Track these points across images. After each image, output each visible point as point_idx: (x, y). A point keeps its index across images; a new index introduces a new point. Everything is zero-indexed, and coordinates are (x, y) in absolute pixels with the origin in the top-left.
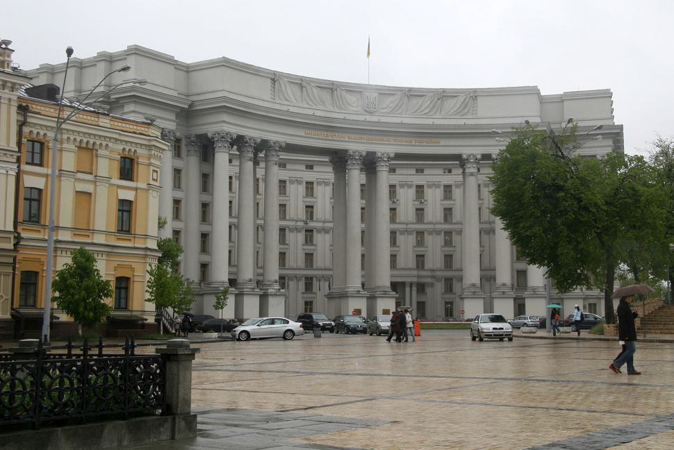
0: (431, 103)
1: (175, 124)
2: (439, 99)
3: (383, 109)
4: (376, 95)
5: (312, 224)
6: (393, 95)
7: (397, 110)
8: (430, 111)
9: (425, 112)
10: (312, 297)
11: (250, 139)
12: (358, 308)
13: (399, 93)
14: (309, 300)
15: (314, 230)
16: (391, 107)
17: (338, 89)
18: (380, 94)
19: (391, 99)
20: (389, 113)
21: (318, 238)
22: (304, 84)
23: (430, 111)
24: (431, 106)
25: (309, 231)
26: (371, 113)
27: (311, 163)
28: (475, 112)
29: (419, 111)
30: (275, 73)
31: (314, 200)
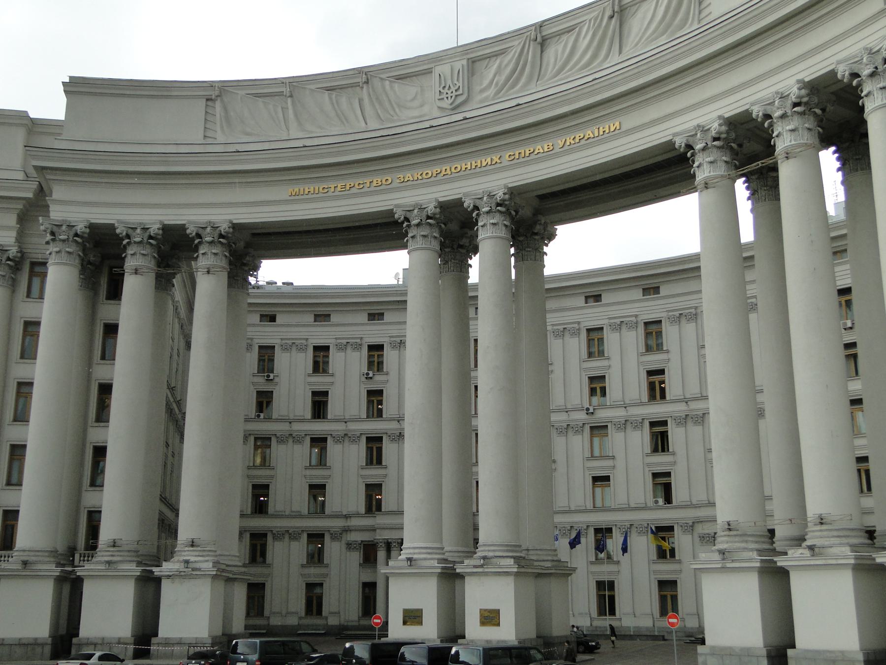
0: (594, 35)
1: (14, 234)
2: (612, 17)
3: (482, 91)
4: (461, 64)
5: (603, 415)
6: (496, 55)
7: (513, 86)
8: (595, 56)
9: (578, 67)
10: (610, 573)
11: (134, 229)
12: (413, 605)
13: (516, 43)
14: (606, 578)
15: (609, 425)
16: (497, 84)
17: (376, 82)
18: (473, 62)
19: (498, 62)
20: (493, 99)
21: (615, 439)
22: (286, 90)
23: (595, 56)
24: (595, 43)
25: (599, 429)
26: (455, 108)
27: (594, 290)
28: (703, 15)
29: (568, 67)
30: (211, 85)
31: (605, 363)
